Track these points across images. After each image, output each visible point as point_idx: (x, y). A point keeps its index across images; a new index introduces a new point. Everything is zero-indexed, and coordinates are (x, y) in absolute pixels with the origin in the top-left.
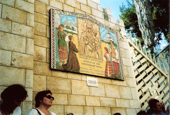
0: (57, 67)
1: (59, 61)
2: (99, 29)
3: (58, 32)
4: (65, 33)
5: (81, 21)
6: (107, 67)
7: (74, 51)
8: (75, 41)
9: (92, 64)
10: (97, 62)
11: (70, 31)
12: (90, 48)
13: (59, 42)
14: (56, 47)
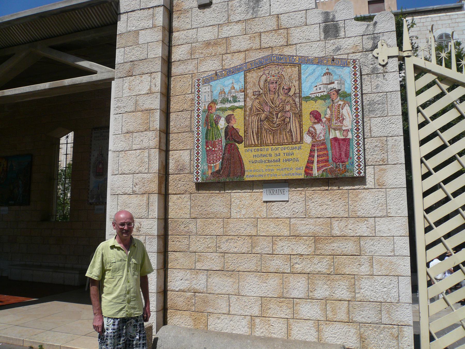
0: (203, 179)
1: (206, 167)
2: (300, 74)
3: (206, 117)
5: (253, 76)
9: (273, 158)
10: (286, 151)
11: (228, 105)
13: (207, 134)
14: (202, 145)
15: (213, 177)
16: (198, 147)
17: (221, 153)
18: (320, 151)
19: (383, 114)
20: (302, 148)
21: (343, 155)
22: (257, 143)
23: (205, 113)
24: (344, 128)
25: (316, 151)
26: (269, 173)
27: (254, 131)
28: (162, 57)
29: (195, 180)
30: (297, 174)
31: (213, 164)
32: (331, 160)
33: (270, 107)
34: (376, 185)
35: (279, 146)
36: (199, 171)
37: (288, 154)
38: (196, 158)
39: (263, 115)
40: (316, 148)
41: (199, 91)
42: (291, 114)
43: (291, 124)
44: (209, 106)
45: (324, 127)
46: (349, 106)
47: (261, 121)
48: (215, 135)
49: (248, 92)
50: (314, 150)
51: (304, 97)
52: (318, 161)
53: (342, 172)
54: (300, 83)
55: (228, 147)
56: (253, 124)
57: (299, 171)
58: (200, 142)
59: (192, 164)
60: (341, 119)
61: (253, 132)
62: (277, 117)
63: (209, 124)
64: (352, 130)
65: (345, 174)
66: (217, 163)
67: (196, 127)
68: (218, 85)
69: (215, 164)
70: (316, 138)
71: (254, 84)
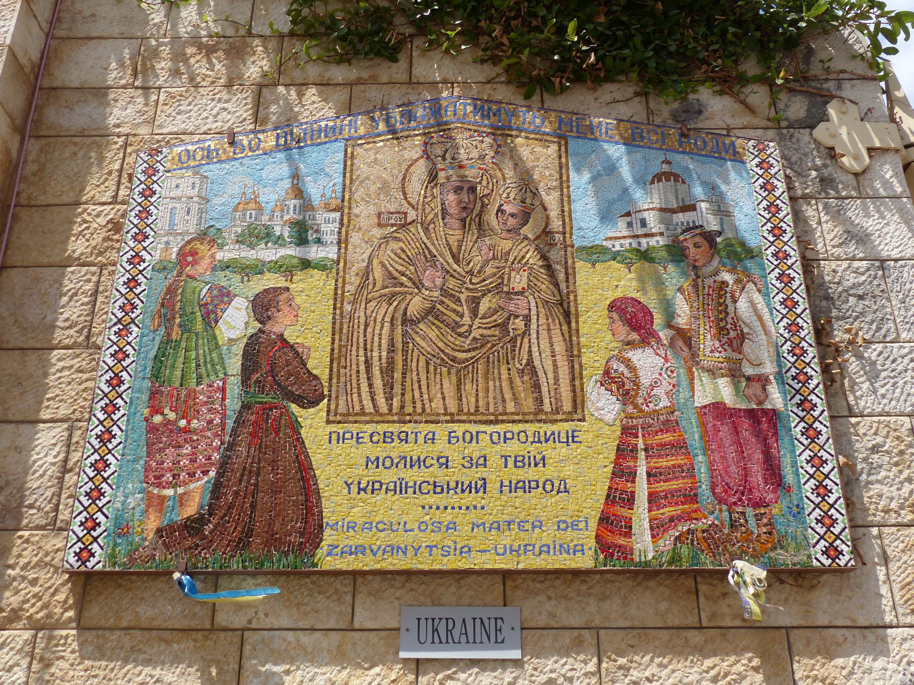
0: (112, 557)
6: (632, 476)
9: (455, 474)
10: (513, 448)
11: (268, 254)
15: (167, 546)
16: (111, 409)
17: (216, 443)
18: (660, 456)
19: (883, 332)
20: (581, 437)
21: (757, 476)
22: (384, 408)
24: (749, 371)
25: (642, 455)
26: (436, 538)
28: (10, 48)
29: (72, 559)
30: (564, 548)
32: (708, 493)
33: (448, 272)
34: (900, 611)
35: (482, 428)
36: (100, 518)
37: (520, 462)
39: (417, 300)
40: (640, 440)
41: (148, 193)
42: (533, 304)
43: (534, 341)
45: (666, 360)
46: (759, 291)
47: (404, 322)
48: (198, 366)
49: (356, 211)
50: (635, 449)
51: (582, 249)
52: (653, 498)
53: (758, 546)
54: (565, 199)
55: (253, 418)
56: (370, 330)
58: (123, 388)
59: (66, 484)
60: (732, 334)
61: (368, 364)
62: (474, 313)
63: (178, 321)
65: (772, 554)
66: (192, 486)
67: (115, 328)
69: (180, 490)
70: (640, 401)
71: (385, 188)
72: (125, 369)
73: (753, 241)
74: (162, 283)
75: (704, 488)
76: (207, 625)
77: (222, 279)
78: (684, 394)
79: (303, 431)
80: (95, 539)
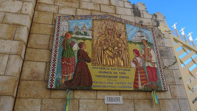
0: (56, 86)
1: (60, 77)
2: (125, 28)
3: (64, 41)
4: (73, 40)
5: (98, 23)
6: (138, 76)
7: (86, 61)
8: (88, 49)
9: (112, 75)
10: (121, 71)
11: (80, 36)
12: (111, 54)
13: (63, 52)
16: (54, 60)
21: (154, 77)
22: (101, 64)
23: (62, 38)
24: (153, 62)
25: (139, 73)
27: (99, 56)
31: (67, 74)
37: (122, 73)
38: (52, 69)
44: (67, 34)
47: (104, 50)
49: (94, 31)
50: (138, 72)
51: (129, 41)
52: (141, 80)
57: (130, 85)
58: (57, 57)
62: (114, 50)
64: (156, 62)
66: (70, 75)
68: (74, 24)
69: (68, 75)
71: (99, 28)
72: (57, 54)
73: (152, 43)
74: (63, 40)
75: (148, 78)
76: (73, 98)
77: (73, 40)
78: (144, 65)
79: (88, 67)
80: (53, 83)
